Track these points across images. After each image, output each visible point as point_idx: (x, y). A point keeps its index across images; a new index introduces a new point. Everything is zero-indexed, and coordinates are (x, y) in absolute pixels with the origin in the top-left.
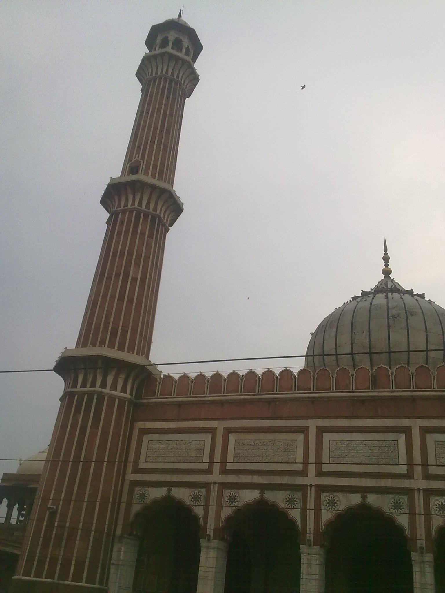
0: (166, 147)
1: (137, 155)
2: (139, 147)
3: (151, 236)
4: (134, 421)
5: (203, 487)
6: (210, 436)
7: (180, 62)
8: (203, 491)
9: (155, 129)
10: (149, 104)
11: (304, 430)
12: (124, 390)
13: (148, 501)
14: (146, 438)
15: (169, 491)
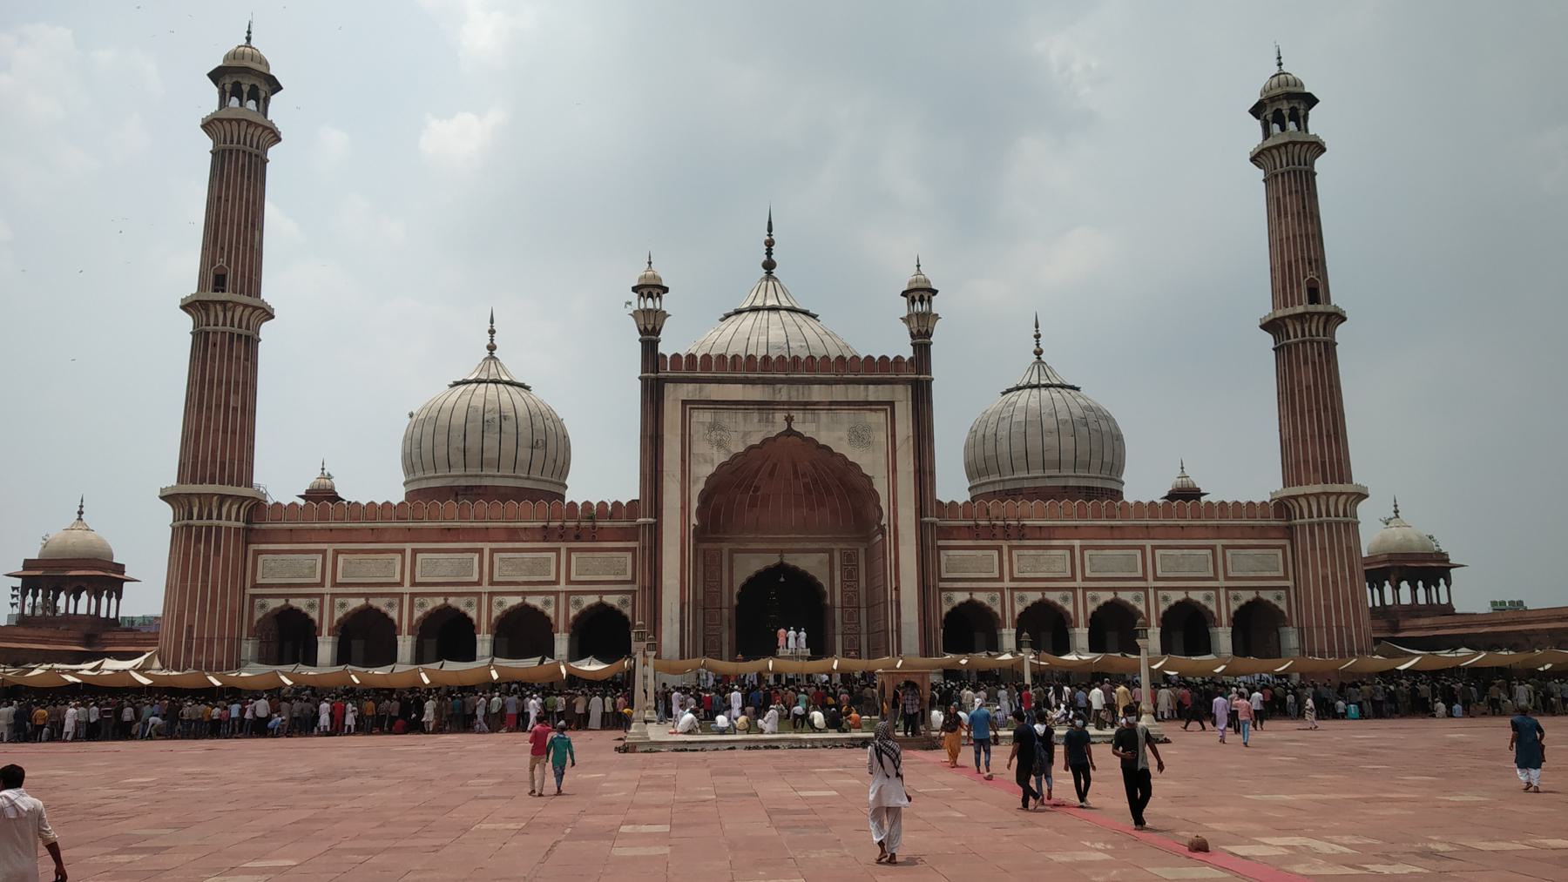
0: (252, 247)
1: (221, 260)
2: (222, 248)
3: (246, 359)
4: (247, 543)
5: (316, 597)
6: (320, 556)
7: (261, 129)
8: (317, 600)
9: (239, 225)
10: (228, 188)
11: (402, 552)
12: (237, 519)
13: (269, 610)
14: (261, 558)
15: (287, 601)
